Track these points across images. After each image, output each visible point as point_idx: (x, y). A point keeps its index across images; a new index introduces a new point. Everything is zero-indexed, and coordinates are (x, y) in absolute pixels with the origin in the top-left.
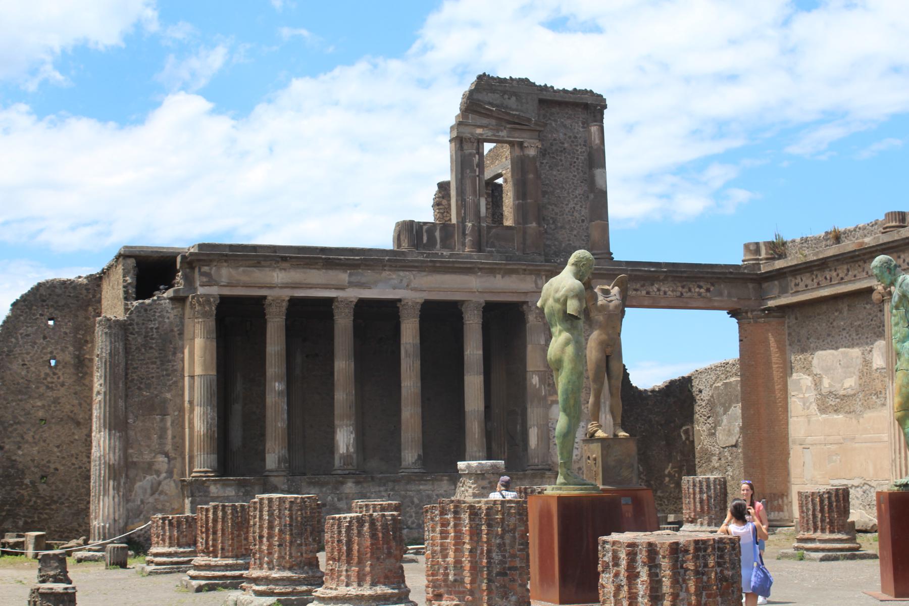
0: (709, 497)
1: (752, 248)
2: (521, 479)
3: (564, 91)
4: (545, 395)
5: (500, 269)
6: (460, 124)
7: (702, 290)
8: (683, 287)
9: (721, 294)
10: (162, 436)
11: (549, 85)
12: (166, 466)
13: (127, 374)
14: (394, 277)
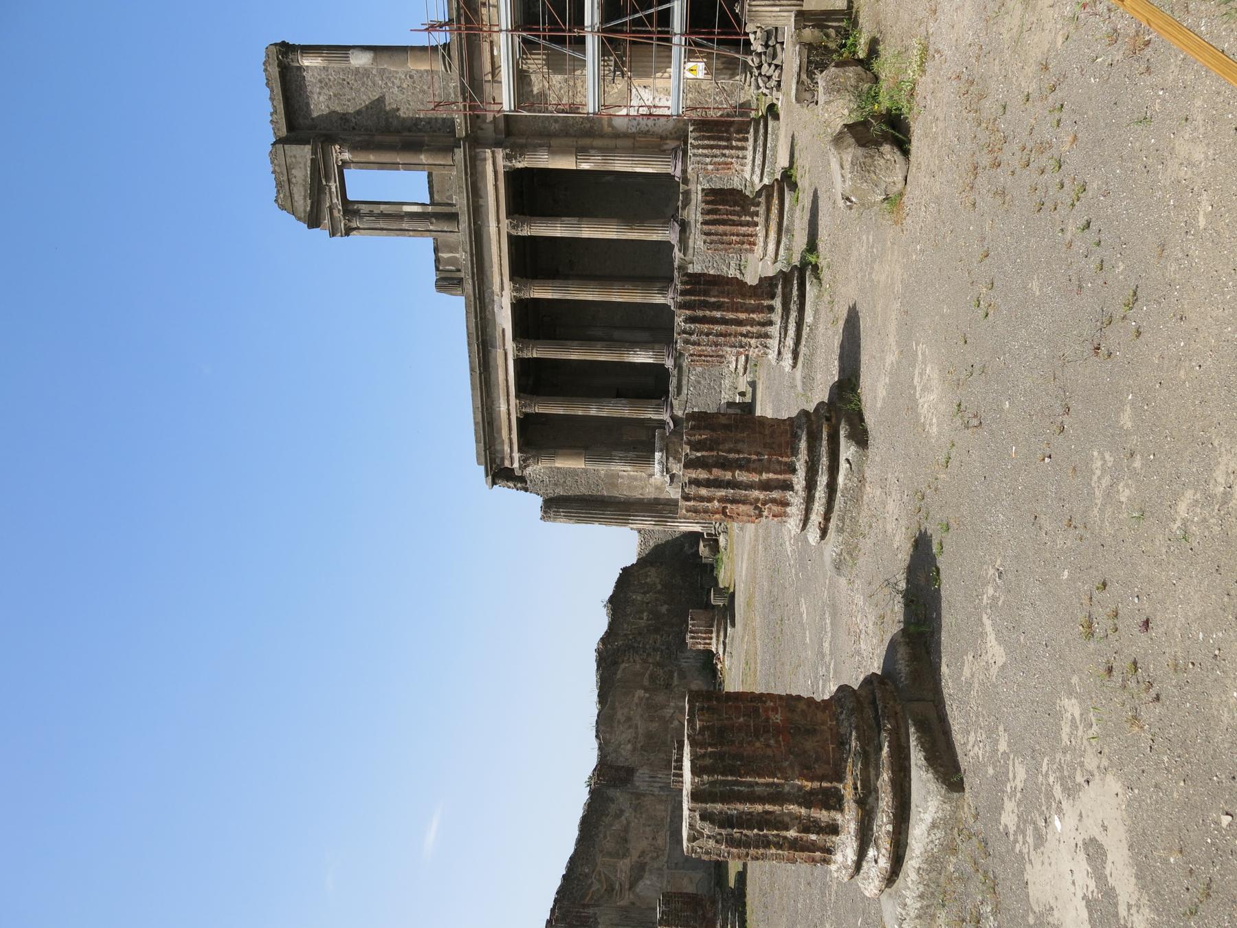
3: (272, 99)
6: (333, 234)
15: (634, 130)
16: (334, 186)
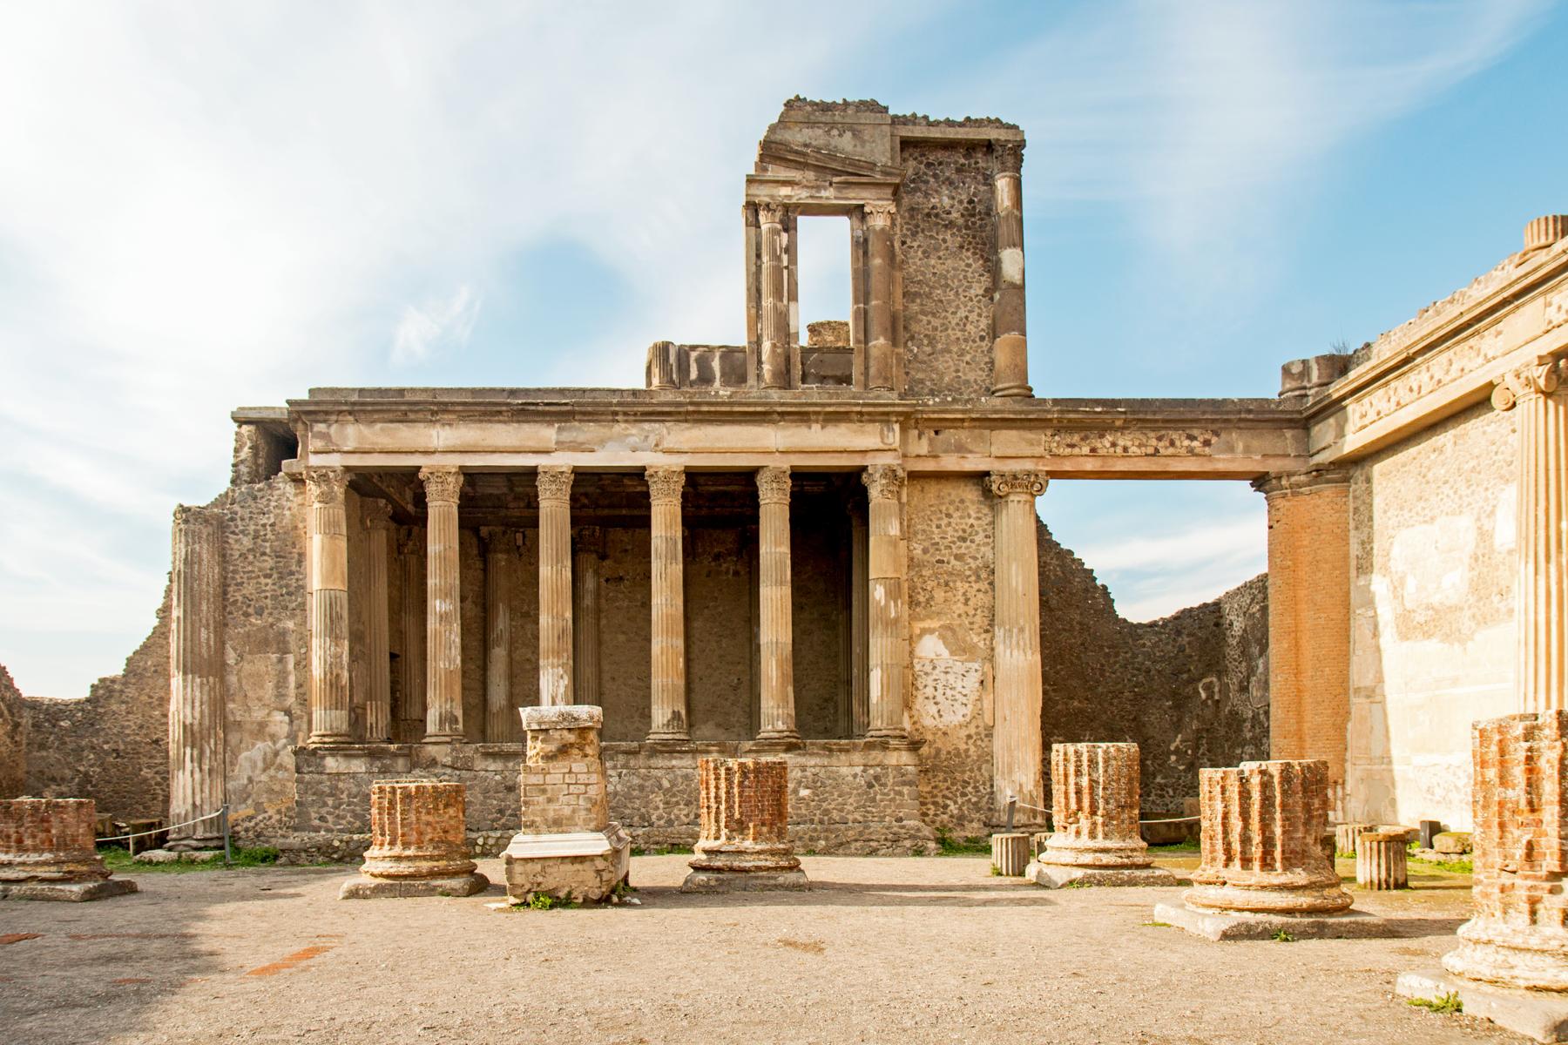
0: (1093, 783)
1: (1296, 370)
2: (848, 751)
4: (896, 621)
5: (818, 413)
7: (1195, 444)
8: (1159, 439)
9: (1231, 449)
10: (281, 683)
11: (920, 115)
12: (286, 728)
13: (225, 593)
15: (917, 667)
16: (829, 195)
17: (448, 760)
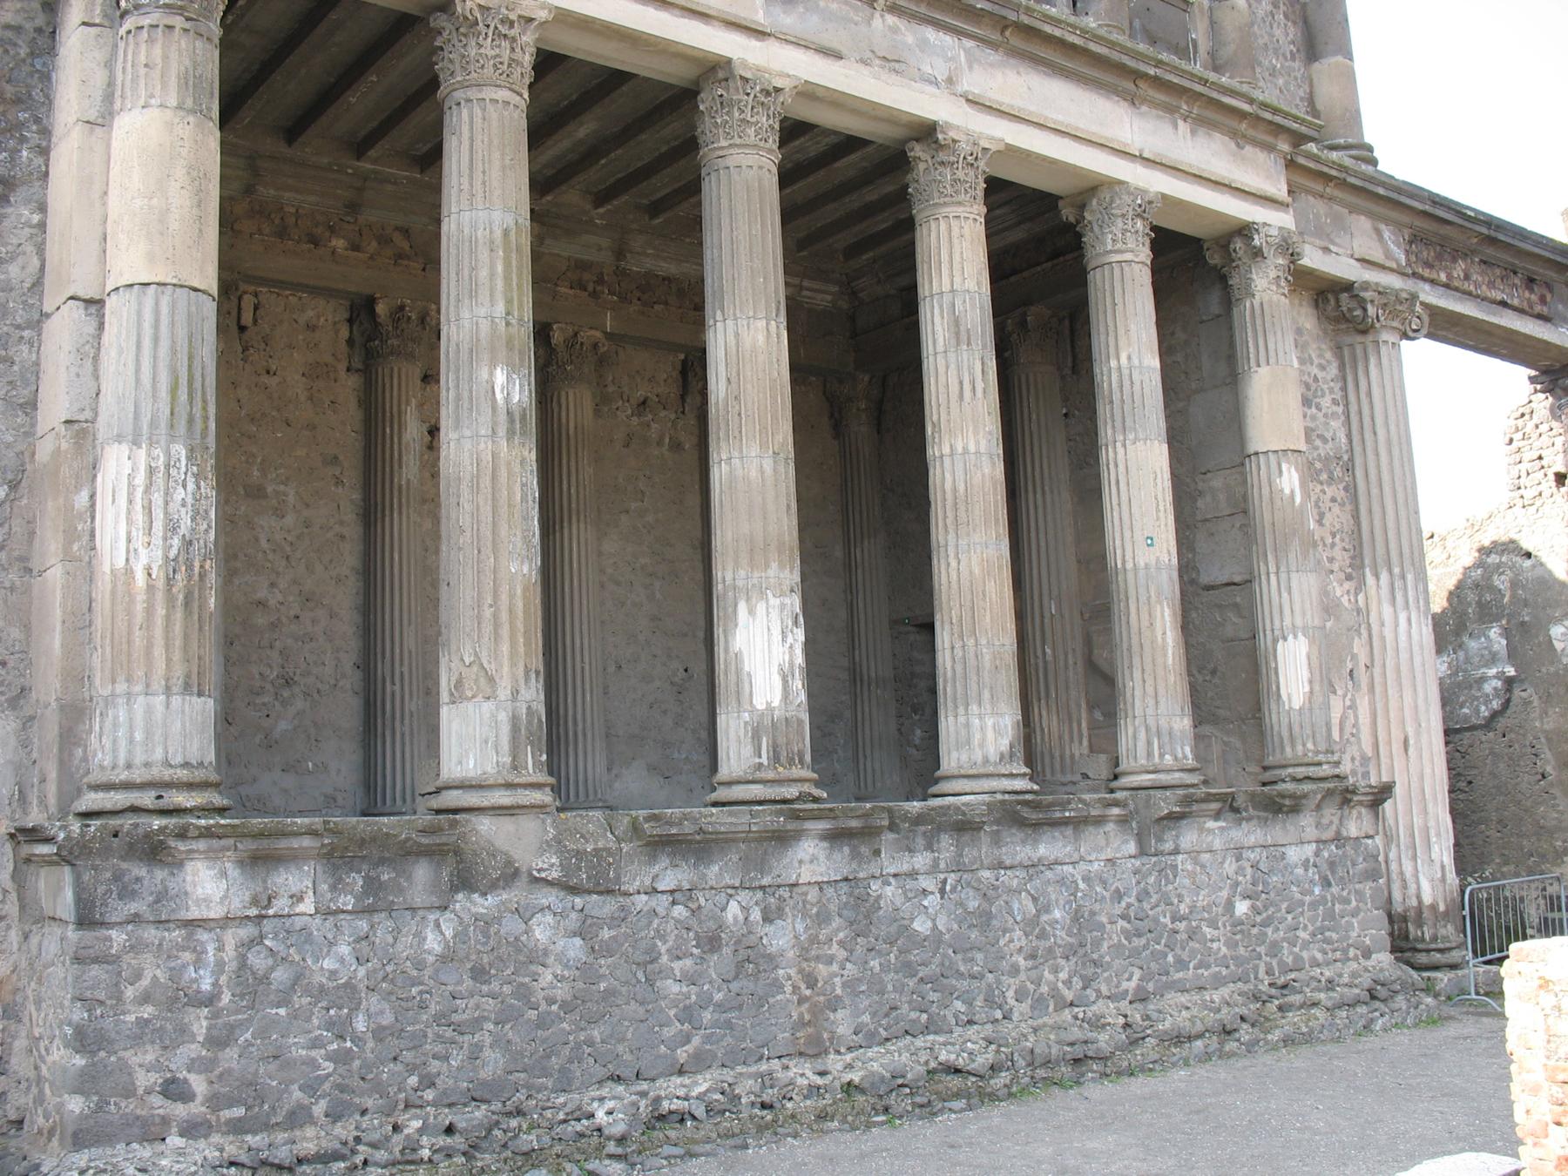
14: (910, 39)
17: (549, 865)
